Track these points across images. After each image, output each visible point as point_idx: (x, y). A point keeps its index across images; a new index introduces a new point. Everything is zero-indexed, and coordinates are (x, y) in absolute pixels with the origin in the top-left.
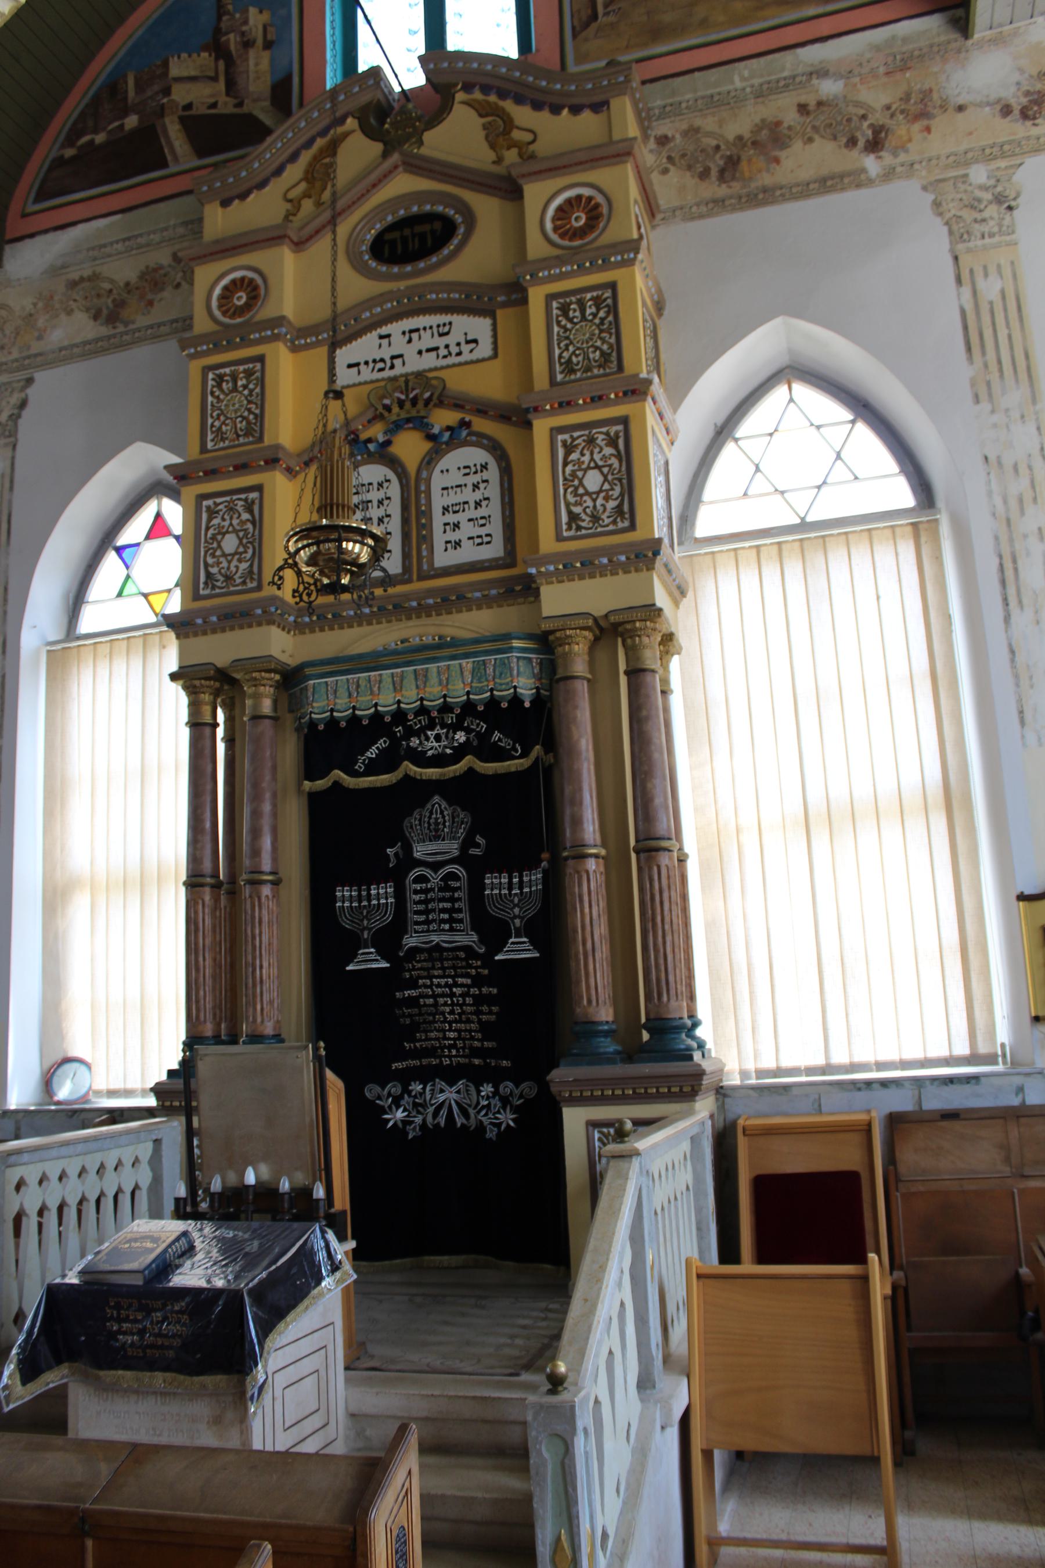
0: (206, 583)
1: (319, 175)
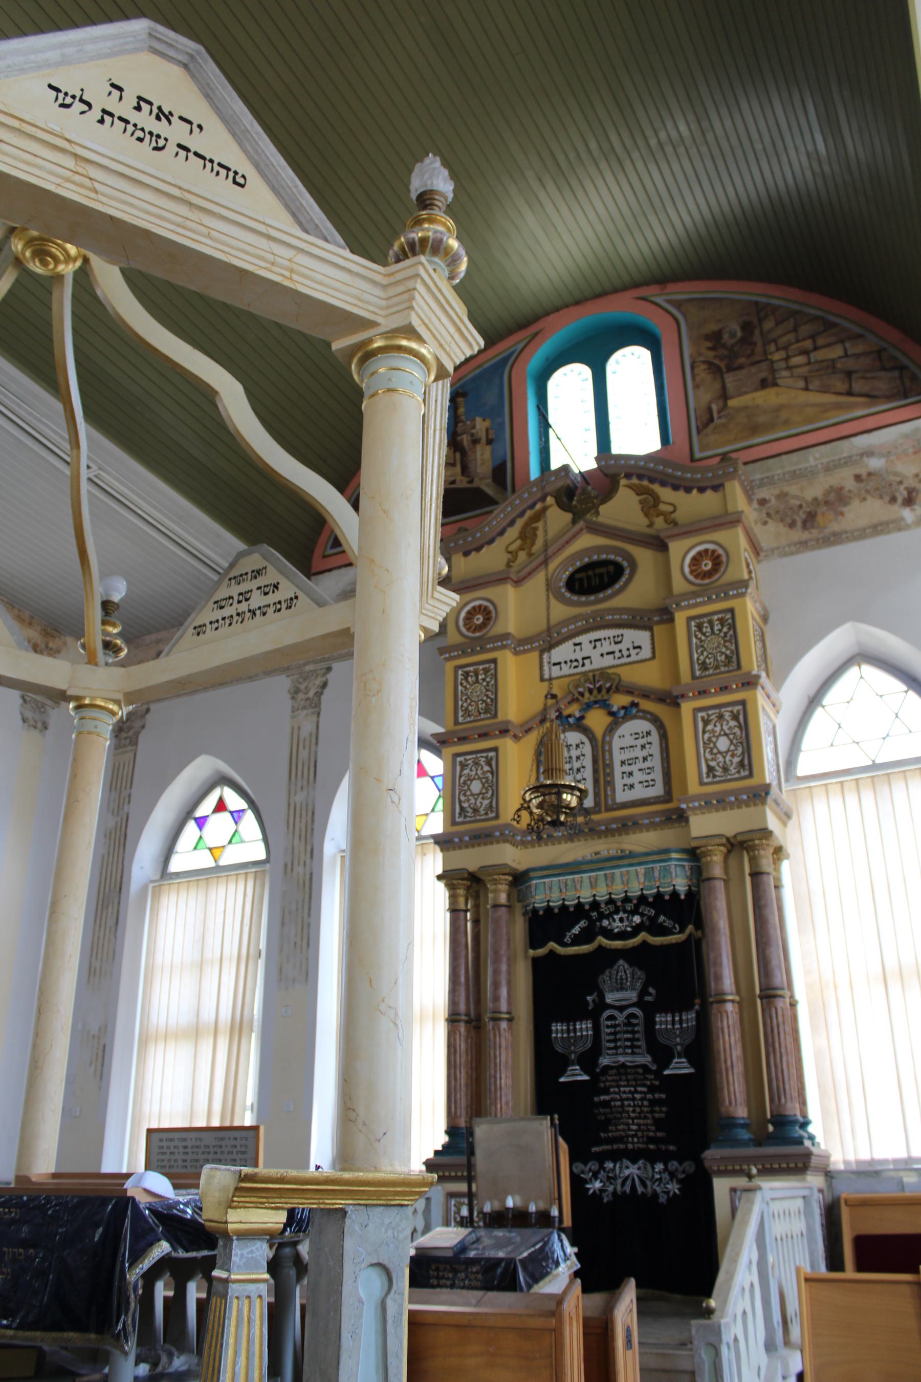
0: (460, 814)
1: (528, 536)
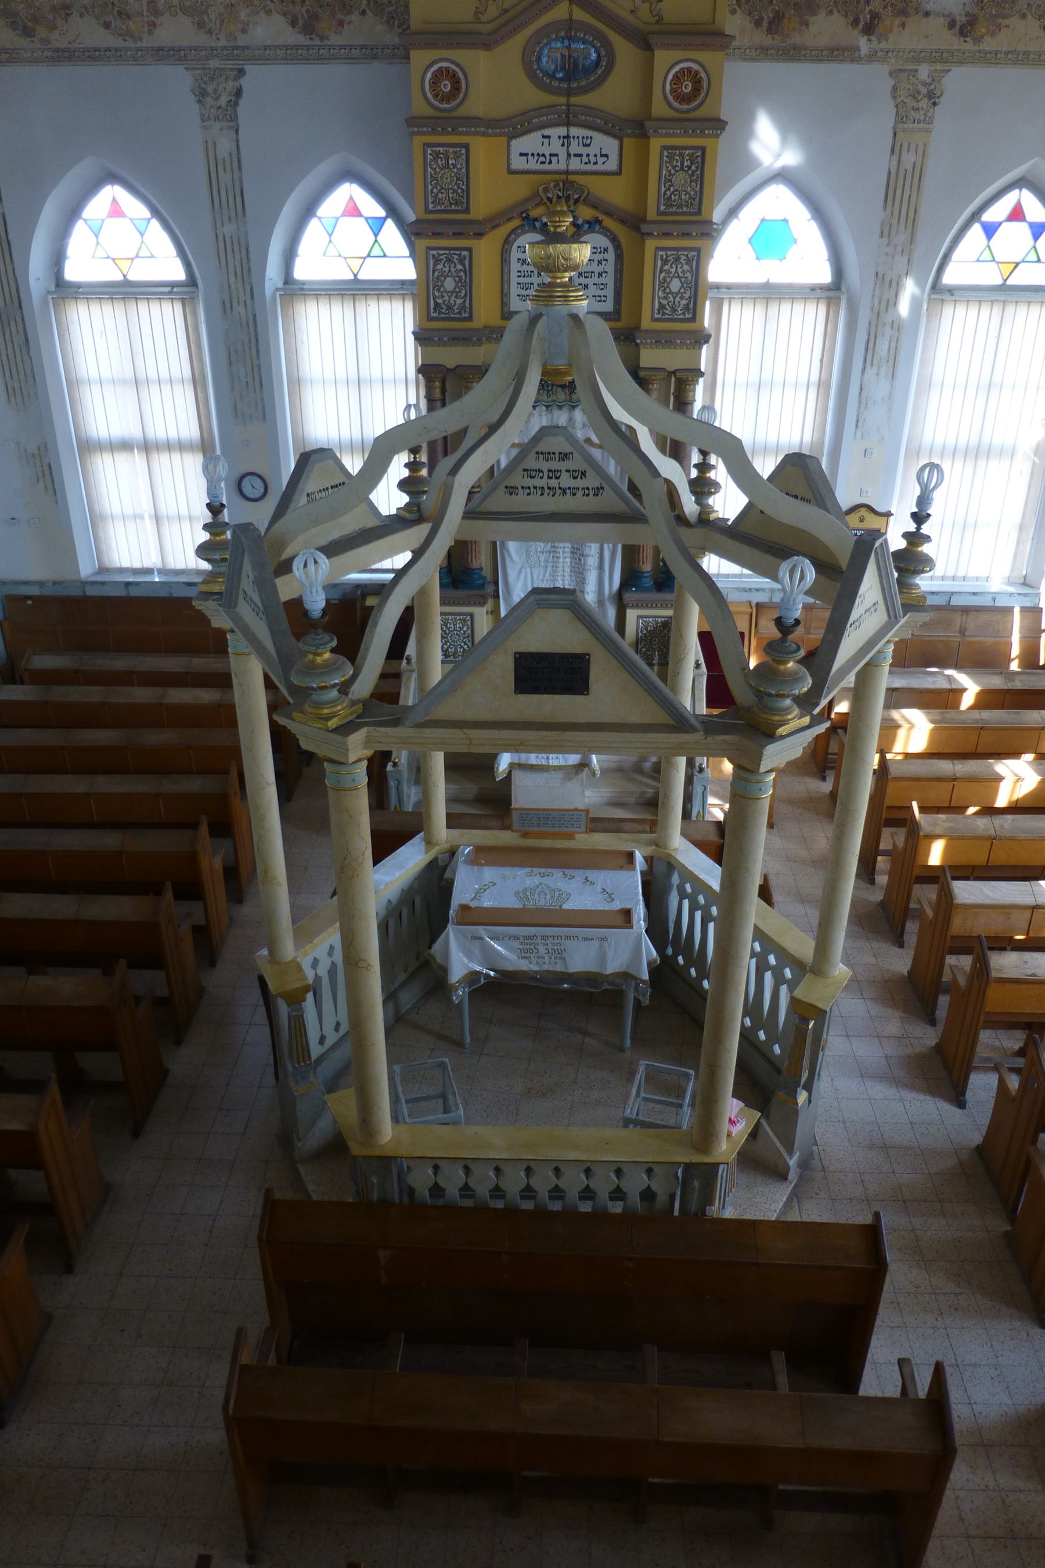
0: (435, 309)
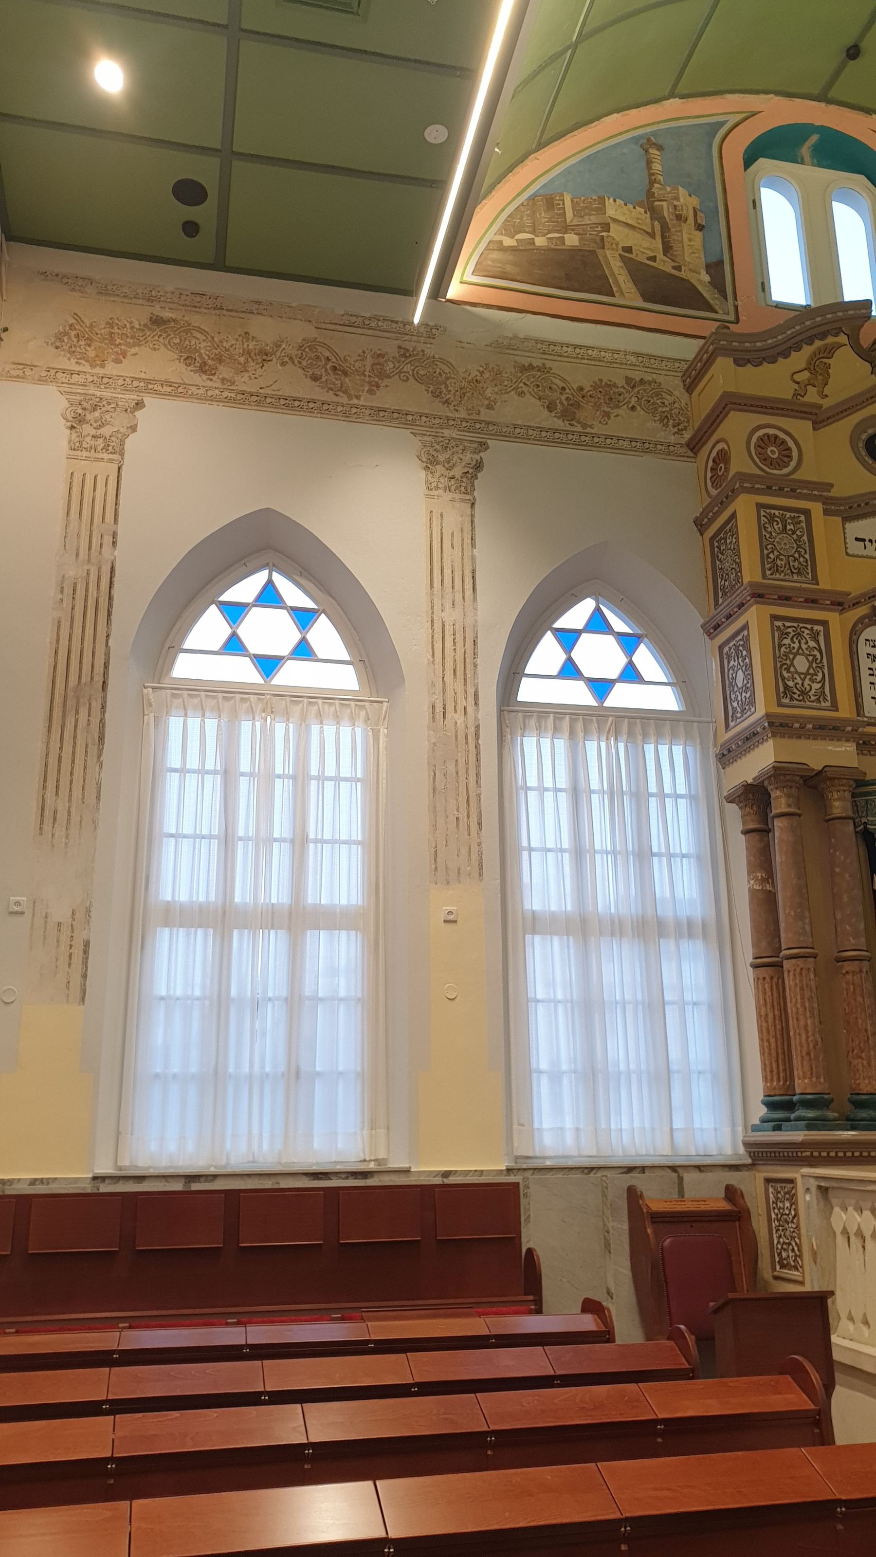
0: (785, 693)
